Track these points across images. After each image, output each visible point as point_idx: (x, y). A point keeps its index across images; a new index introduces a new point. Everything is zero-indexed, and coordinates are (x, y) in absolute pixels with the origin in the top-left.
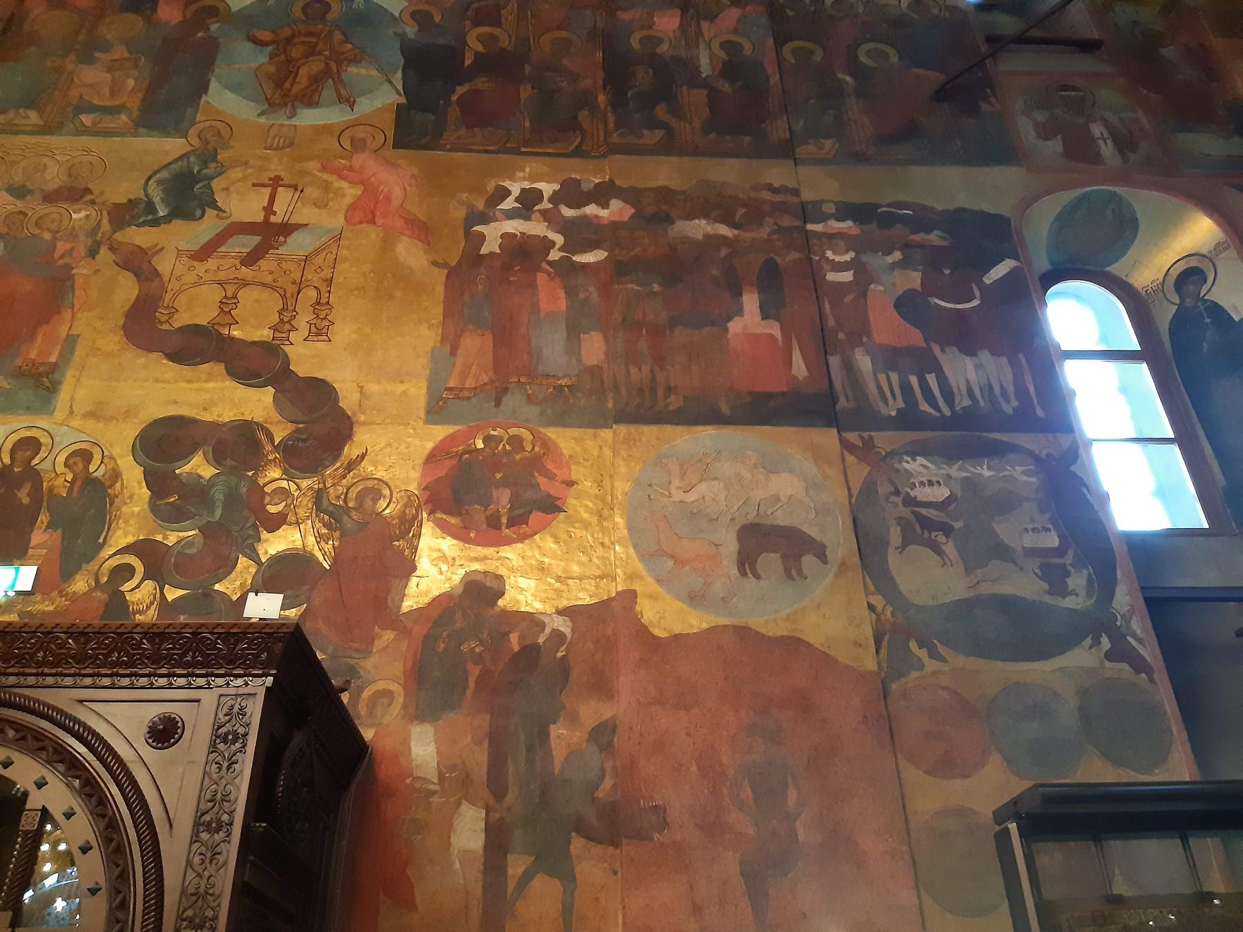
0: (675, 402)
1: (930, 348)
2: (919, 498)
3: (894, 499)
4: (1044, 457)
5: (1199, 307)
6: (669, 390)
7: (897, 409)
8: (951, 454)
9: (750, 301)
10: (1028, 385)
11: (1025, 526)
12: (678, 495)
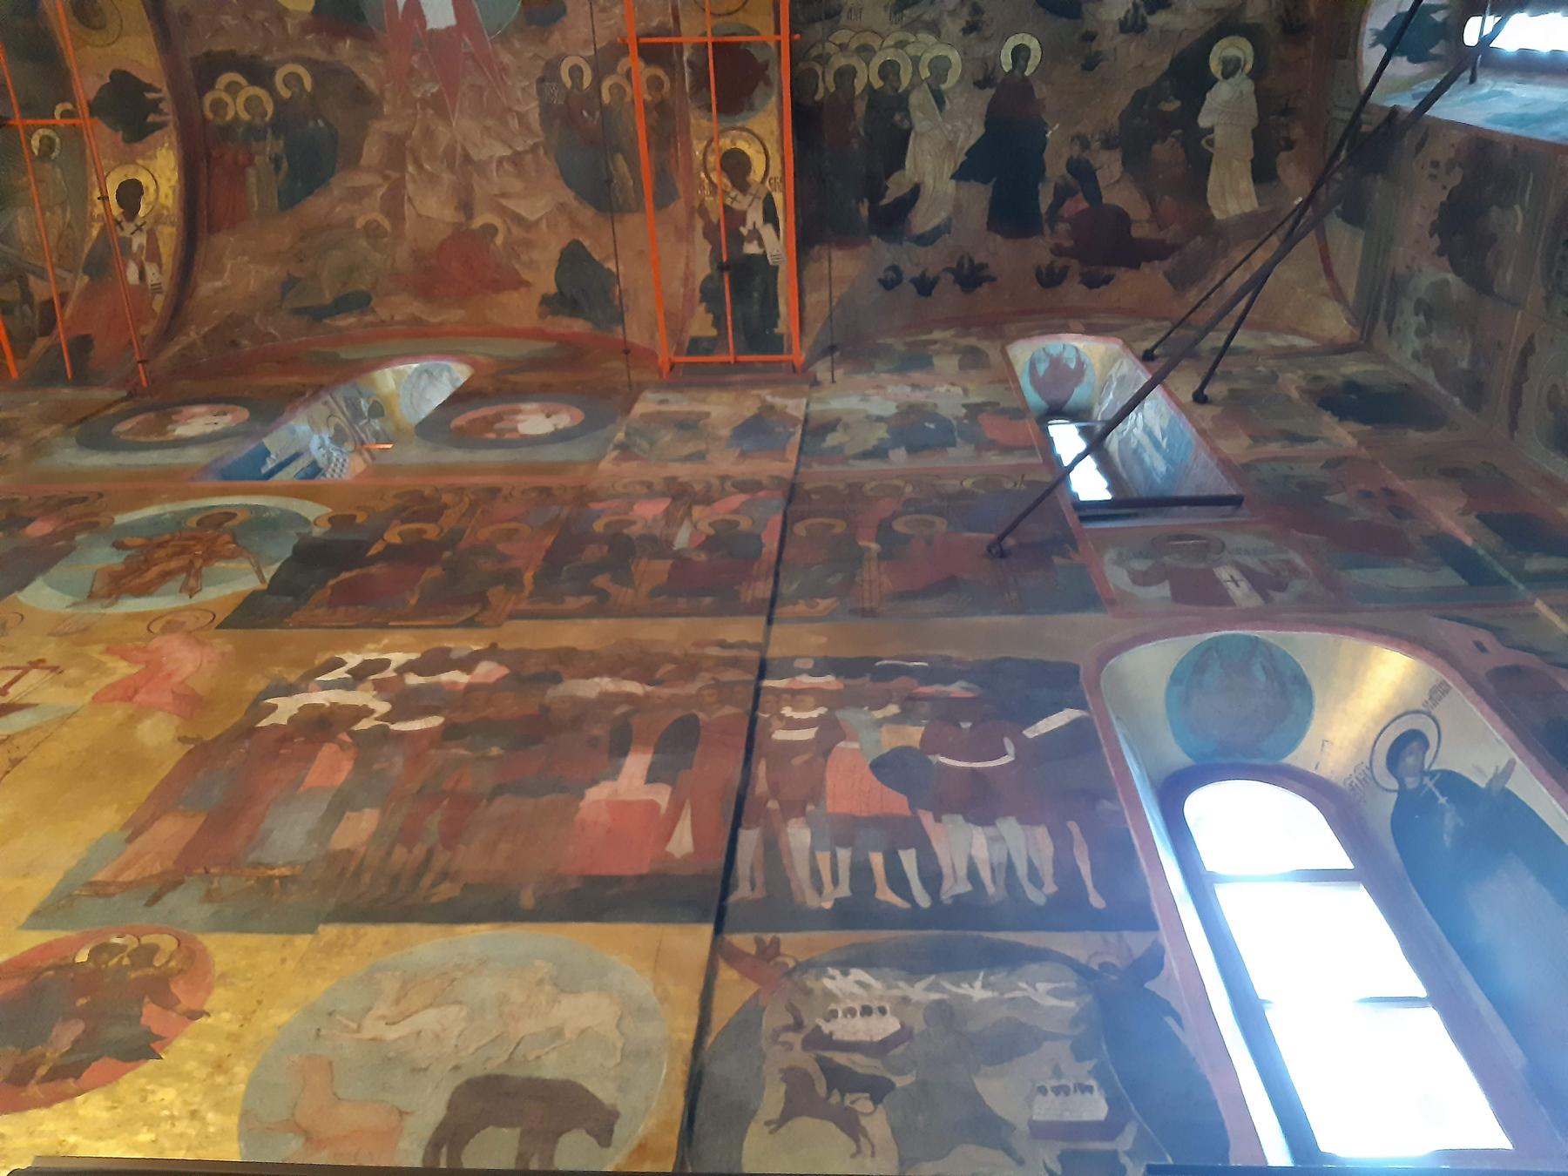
0: (446, 891)
1: (917, 820)
2: (838, 1036)
3: (790, 1037)
4: (1096, 968)
5: (1426, 785)
6: (445, 876)
7: (836, 900)
8: (914, 965)
9: (636, 764)
10: (1079, 863)
11: (1041, 1083)
12: (372, 1028)
